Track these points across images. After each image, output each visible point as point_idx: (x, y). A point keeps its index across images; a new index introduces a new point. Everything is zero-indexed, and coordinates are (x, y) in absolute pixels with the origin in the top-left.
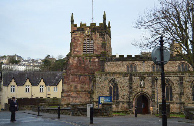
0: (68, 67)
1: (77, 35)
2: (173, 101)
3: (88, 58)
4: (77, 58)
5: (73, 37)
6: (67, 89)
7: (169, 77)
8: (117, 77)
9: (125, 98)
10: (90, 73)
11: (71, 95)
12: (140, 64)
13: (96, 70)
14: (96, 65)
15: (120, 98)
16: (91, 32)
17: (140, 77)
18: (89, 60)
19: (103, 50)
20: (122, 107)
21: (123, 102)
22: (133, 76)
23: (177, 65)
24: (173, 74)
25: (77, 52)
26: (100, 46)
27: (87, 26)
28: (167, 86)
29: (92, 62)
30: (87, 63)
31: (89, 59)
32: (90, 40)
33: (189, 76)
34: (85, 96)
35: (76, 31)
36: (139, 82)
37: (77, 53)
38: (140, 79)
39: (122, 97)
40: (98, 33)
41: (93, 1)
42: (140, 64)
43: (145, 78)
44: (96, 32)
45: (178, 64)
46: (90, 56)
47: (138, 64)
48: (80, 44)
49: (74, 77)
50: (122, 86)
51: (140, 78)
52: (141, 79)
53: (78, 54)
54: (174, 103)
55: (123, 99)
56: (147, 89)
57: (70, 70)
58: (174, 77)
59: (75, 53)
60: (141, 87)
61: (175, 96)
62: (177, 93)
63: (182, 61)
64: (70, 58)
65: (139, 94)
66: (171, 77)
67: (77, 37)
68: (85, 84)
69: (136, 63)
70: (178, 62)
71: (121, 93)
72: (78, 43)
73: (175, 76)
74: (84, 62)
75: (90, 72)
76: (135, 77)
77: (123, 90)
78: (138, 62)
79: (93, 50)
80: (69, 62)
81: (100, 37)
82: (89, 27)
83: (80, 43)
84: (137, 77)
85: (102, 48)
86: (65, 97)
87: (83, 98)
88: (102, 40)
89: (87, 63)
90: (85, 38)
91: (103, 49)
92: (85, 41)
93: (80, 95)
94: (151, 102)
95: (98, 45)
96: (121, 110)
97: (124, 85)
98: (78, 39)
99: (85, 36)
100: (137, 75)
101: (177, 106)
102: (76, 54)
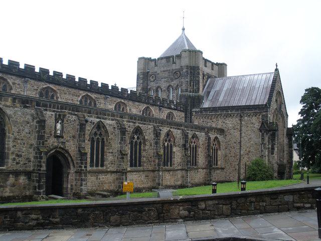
2: (105, 168)
7: (103, 119)
8: (7, 106)
9: (22, 163)
12: (19, 84)
15: (10, 161)
17: (57, 112)
20: (13, 185)
21: (17, 174)
22: (42, 109)
23: (79, 99)
24: (109, 115)
28: (98, 138)
33: (129, 122)
36: (54, 124)
38: (56, 117)
39: (14, 159)
42: (19, 84)
43: (64, 116)
45: (81, 97)
47: (14, 84)
50: (15, 129)
51: (56, 114)
52: (57, 117)
54: (108, 172)
55: (17, 163)
56: (68, 141)
58: (109, 119)
60: (57, 137)
61: (109, 158)
62: (112, 153)
63: (87, 93)
65: (51, 152)
66: (105, 119)
69: (11, 80)
70: (83, 93)
71: (12, 149)
73: (112, 120)
76: (46, 110)
77: (19, 141)
78: (14, 77)
84: (50, 111)
94: (72, 170)
96: (11, 194)
97: (21, 128)
100: (50, 107)
101: (110, 178)
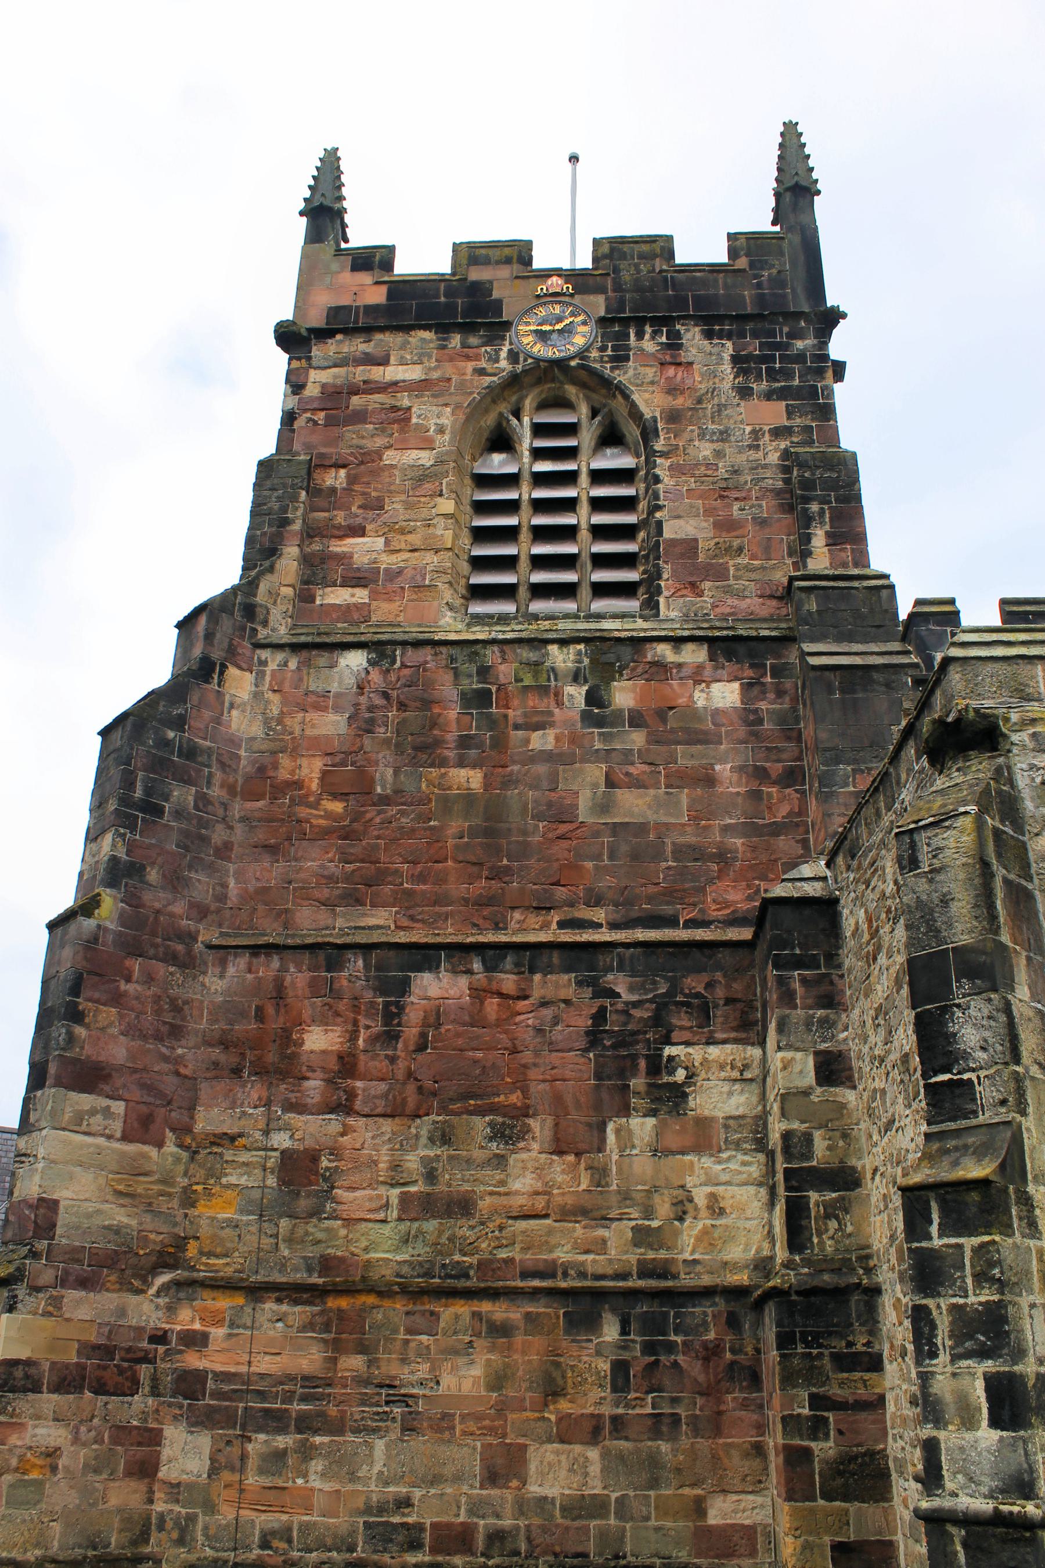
0: (182, 795)
1: (384, 362)
3: (561, 658)
4: (355, 660)
5: (312, 390)
6: (120, 1216)
10: (600, 915)
11: (193, 1361)
13: (723, 857)
14: (709, 780)
16: (602, 321)
18: (576, 694)
19: (820, 561)
25: (357, 579)
26: (766, 507)
27: (539, 262)
29: (636, 720)
30: (542, 741)
31: (576, 677)
32: (586, 438)
34: (497, 1381)
35: (370, 309)
37: (361, 595)
40: (709, 335)
41: (574, 159)
44: (692, 337)
46: (596, 641)
48: (422, 476)
49: (279, 993)
53: (384, 611)
57: (224, 851)
59: (339, 596)
64: (232, 655)
67: (370, 387)
68: (498, 1134)
72: (390, 457)
74: (492, 723)
75: (595, 900)
79: (631, 576)
80: (218, 721)
81: (744, 392)
82: (572, 276)
83: (426, 458)
85: (807, 521)
86: (49, 1401)
87: (443, 1424)
88: (778, 433)
89: (542, 741)
90: (504, 408)
91: (819, 540)
92: (497, 458)
93: (390, 1367)
95: (723, 492)
98: (400, 417)
99: (514, 382)
102: (346, 611)
